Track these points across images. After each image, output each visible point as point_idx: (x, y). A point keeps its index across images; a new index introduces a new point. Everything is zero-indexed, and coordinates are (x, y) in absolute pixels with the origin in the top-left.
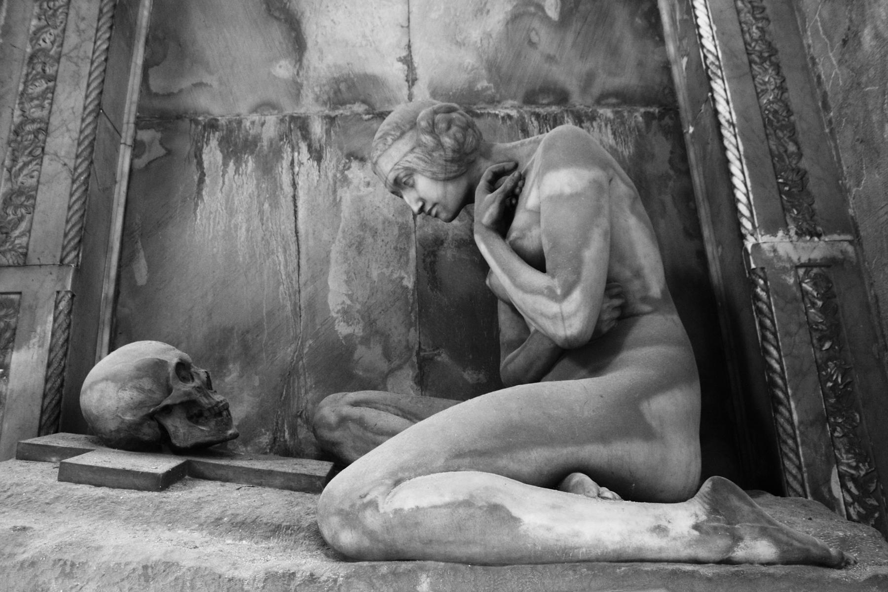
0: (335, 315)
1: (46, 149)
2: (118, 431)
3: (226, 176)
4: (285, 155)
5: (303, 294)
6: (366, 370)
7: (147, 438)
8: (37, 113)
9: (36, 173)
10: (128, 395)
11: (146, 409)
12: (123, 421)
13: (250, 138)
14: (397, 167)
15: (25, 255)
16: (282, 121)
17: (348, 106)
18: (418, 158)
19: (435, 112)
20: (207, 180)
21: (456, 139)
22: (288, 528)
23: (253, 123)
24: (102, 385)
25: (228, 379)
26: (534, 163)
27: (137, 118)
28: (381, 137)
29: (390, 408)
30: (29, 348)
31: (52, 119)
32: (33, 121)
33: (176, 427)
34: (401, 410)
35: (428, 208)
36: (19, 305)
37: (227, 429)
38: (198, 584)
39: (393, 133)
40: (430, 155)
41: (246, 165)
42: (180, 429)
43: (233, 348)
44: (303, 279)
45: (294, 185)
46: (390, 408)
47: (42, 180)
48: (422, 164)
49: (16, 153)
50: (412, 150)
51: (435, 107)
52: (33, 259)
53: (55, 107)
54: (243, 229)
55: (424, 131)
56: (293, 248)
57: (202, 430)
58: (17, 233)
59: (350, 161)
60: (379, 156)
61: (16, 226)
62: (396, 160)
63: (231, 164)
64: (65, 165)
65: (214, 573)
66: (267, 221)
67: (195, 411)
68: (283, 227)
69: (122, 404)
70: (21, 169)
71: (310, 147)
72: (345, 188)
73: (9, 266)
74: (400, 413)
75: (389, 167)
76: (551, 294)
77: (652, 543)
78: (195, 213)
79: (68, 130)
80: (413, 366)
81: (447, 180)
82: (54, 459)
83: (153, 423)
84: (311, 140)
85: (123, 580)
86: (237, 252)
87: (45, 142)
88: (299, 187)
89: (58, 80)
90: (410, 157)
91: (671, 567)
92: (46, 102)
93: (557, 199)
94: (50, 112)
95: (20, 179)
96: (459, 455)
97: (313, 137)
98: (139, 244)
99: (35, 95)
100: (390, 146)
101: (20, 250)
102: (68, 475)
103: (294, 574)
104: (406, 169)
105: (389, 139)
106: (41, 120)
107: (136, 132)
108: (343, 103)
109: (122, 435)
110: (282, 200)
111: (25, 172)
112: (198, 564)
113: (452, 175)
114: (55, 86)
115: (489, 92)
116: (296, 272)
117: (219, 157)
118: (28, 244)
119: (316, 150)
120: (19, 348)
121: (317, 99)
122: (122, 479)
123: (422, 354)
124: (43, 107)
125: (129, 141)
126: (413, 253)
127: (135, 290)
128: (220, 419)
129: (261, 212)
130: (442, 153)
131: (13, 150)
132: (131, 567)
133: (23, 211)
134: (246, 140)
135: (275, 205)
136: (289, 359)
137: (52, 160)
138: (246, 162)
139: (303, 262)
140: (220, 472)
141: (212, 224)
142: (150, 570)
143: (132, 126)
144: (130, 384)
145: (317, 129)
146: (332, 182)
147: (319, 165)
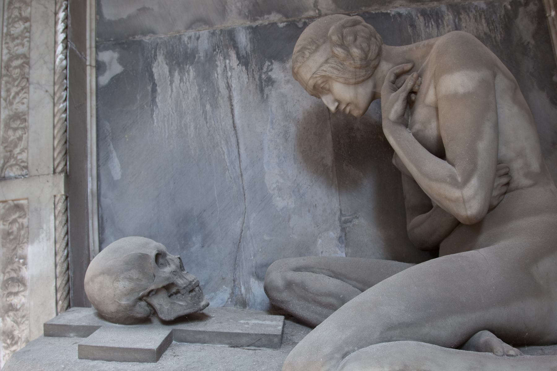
0: (272, 192)
1: (31, 80)
2: (117, 312)
3: (174, 84)
4: (218, 63)
5: (245, 177)
7: (139, 316)
8: (21, 50)
10: (122, 285)
11: (136, 293)
12: (120, 305)
13: (189, 51)
14: (315, 76)
15: (26, 168)
16: (213, 34)
17: (266, 16)
18: (332, 67)
19: (343, 26)
20: (159, 90)
21: (362, 49)
23: (190, 38)
26: (431, 64)
27: (96, 42)
28: (299, 51)
29: (324, 271)
30: (40, 242)
31: (32, 54)
32: (17, 57)
33: (161, 305)
34: (333, 272)
35: (343, 107)
36: (28, 208)
37: (200, 302)
39: (309, 47)
40: (342, 64)
41: (189, 74)
42: (165, 306)
44: (243, 165)
45: (229, 87)
46: (324, 271)
48: (336, 72)
50: (326, 61)
51: (342, 22)
52: (33, 172)
53: (32, 44)
54: (192, 128)
55: (335, 45)
56: (233, 140)
58: (17, 150)
59: (272, 63)
60: (300, 67)
61: (16, 146)
62: (314, 70)
63: (176, 74)
64: (47, 91)
66: (210, 119)
67: (174, 290)
68: (223, 123)
69: (118, 292)
70: (14, 98)
71: (238, 54)
72: (270, 87)
73: (16, 178)
75: (308, 76)
76: (454, 183)
78: (152, 117)
79: (45, 63)
81: (357, 83)
82: (72, 335)
83: (143, 303)
86: (189, 146)
87: (29, 74)
88: (233, 89)
90: (326, 67)
92: (25, 40)
93: (454, 98)
94: (29, 48)
95: (14, 107)
96: (391, 328)
97: (239, 46)
98: (112, 146)
99: (15, 35)
100: (308, 58)
101: (23, 164)
102: (86, 353)
104: (323, 77)
105: (307, 53)
106: (24, 56)
108: (261, 14)
109: (120, 315)
110: (221, 102)
111: (18, 100)
113: (361, 79)
114: (31, 26)
116: (238, 159)
117: (166, 69)
118: (27, 159)
119: (243, 56)
120: (33, 242)
121: (240, 13)
124: (23, 45)
125: (94, 64)
126: (329, 136)
127: (113, 184)
128: (194, 293)
129: (205, 112)
130: (352, 62)
134: (186, 53)
135: (215, 106)
137: (36, 89)
138: (188, 72)
139: (242, 151)
140: (198, 337)
141: (166, 125)
143: (94, 49)
144: (122, 276)
146: (258, 83)
147: (247, 69)
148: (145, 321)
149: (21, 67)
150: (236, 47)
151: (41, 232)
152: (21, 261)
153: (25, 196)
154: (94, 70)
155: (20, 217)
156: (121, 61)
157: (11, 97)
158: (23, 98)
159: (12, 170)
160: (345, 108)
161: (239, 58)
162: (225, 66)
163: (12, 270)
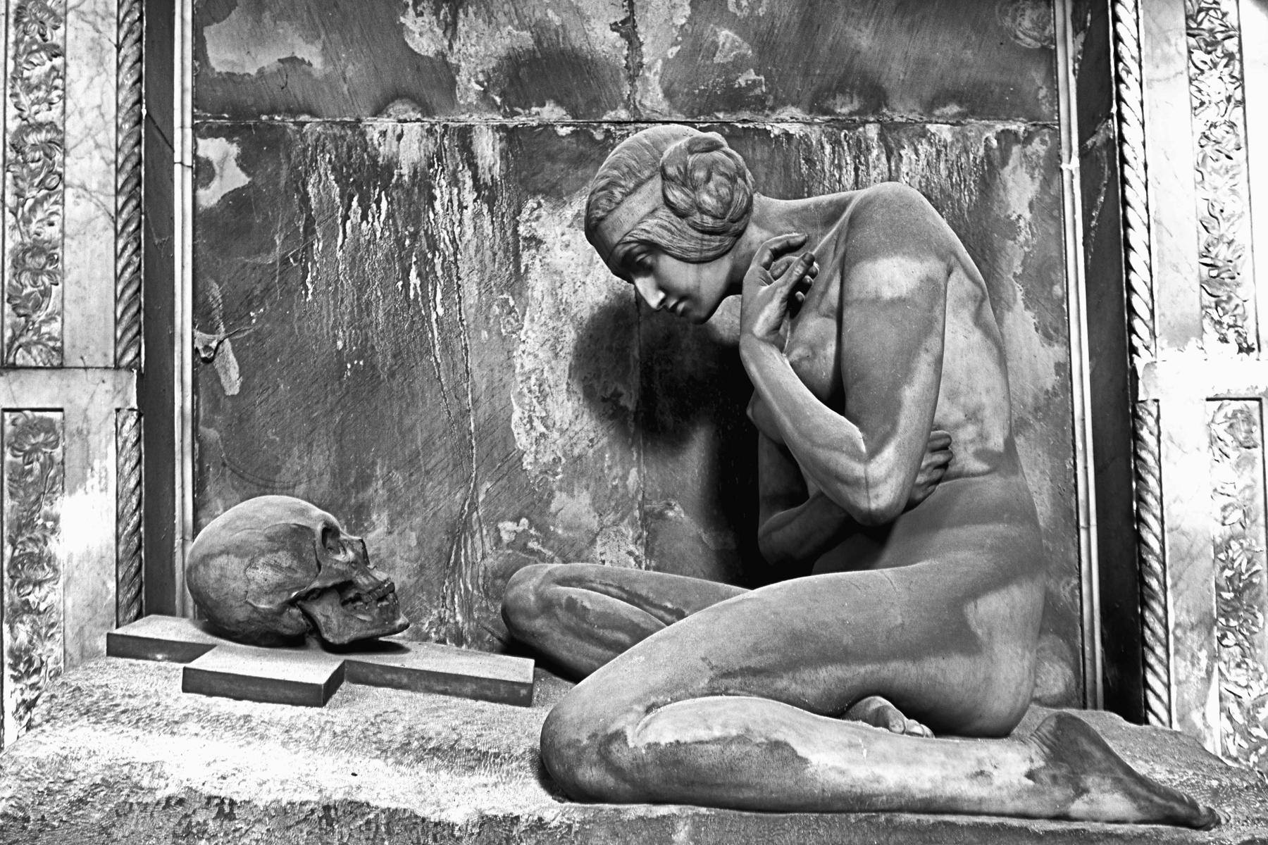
6: (568, 528)
7: (288, 632)
9: (53, 218)
12: (255, 609)
16: (430, 132)
17: (534, 110)
22: (497, 755)
23: (383, 134)
24: (222, 560)
25: (371, 536)
29: (610, 589)
32: (39, 127)
38: (396, 829)
43: (376, 491)
47: (68, 230)
49: (20, 183)
57: (364, 621)
65: (416, 817)
70: (33, 209)
71: (475, 178)
74: (625, 596)
77: (972, 791)
80: (633, 524)
83: (295, 611)
84: (476, 166)
85: (298, 823)
87: (63, 165)
89: (68, 54)
91: (995, 820)
95: (33, 227)
97: (480, 163)
103: (517, 818)
107: (195, 143)
111: (40, 215)
112: (393, 806)
115: (758, 91)
118: (62, 333)
119: (485, 184)
122: (270, 691)
123: (647, 507)
125: (188, 161)
128: (385, 603)
131: (15, 178)
132: (308, 807)
133: (46, 279)
136: (457, 509)
137: (78, 197)
142: (333, 812)
143: (189, 131)
145: (487, 149)
148: (293, 642)
149: (48, 147)
150: (471, 161)
151: (89, 475)
152: (49, 524)
153: (58, 406)
154: (189, 174)
155: (46, 444)
156: (245, 162)
157: (27, 207)
158: (52, 214)
159: (29, 352)
160: (675, 306)
161: (477, 186)
162: (451, 201)
163: (30, 539)
